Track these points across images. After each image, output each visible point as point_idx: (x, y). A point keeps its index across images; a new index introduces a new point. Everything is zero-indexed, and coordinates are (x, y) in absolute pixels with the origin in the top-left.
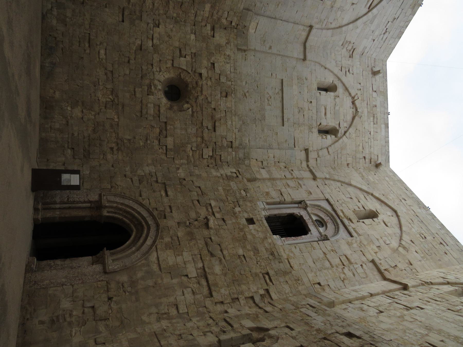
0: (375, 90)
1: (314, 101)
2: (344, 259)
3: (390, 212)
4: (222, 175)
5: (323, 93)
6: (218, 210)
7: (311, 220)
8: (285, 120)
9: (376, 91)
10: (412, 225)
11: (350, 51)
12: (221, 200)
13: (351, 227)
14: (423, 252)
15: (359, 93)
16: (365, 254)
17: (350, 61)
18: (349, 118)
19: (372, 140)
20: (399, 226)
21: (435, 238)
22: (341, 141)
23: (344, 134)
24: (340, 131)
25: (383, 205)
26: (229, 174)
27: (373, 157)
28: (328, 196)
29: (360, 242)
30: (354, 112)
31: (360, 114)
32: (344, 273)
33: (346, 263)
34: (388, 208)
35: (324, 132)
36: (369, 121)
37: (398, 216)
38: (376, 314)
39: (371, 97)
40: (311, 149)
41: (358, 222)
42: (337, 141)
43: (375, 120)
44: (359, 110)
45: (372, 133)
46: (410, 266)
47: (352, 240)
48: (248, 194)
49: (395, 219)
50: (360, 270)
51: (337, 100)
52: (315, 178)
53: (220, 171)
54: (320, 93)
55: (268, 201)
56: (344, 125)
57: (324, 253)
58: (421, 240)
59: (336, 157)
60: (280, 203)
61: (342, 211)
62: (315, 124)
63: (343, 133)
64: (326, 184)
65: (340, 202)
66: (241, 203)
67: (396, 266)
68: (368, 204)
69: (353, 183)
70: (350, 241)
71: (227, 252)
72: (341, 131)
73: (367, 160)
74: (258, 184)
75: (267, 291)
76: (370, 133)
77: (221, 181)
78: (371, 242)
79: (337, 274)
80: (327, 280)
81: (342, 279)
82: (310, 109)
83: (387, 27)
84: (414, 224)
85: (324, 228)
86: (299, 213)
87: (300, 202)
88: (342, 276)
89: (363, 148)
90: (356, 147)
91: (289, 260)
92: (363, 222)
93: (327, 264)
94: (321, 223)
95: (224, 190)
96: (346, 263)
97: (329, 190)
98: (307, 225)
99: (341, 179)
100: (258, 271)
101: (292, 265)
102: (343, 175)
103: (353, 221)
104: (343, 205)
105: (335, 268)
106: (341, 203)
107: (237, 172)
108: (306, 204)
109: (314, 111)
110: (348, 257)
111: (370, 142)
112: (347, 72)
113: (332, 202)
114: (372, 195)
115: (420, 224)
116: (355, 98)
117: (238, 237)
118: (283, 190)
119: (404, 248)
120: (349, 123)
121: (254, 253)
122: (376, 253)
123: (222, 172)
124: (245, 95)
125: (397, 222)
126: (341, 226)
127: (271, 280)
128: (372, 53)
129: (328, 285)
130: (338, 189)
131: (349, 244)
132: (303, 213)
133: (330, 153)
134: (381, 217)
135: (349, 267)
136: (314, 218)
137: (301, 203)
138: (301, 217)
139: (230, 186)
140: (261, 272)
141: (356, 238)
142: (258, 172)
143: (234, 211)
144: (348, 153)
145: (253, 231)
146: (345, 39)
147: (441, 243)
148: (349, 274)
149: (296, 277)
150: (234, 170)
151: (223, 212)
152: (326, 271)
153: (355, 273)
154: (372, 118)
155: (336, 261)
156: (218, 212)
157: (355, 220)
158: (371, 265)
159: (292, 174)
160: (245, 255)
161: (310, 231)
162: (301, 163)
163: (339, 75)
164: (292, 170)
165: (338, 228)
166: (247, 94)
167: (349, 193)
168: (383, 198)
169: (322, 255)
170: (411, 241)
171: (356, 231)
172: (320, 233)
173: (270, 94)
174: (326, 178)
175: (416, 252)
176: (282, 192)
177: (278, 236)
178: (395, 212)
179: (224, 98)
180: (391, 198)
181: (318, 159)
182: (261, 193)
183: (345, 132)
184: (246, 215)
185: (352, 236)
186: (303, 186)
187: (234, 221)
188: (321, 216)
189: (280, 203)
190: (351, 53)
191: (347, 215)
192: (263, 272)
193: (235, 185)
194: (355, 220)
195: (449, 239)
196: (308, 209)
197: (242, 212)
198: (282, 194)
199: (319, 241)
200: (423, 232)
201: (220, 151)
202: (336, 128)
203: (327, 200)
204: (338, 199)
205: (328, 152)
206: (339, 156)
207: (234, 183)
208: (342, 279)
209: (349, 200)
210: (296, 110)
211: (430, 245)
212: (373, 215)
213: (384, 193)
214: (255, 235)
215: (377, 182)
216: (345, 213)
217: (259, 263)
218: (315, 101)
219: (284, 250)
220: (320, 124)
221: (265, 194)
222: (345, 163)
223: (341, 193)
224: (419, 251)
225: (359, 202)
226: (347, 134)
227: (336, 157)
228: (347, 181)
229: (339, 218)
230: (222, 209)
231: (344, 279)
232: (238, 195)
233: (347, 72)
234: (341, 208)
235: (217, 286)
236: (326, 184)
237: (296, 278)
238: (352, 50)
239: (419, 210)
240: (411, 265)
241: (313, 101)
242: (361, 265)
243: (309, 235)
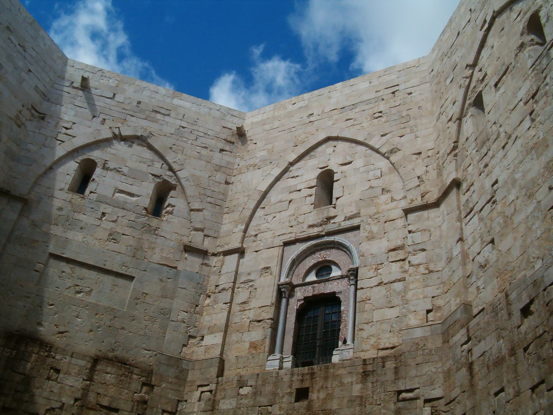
0: (111, 96)
1: (104, 208)
2: (394, 256)
3: (327, 148)
5: (91, 186)
7: (316, 285)
8: (123, 272)
9: (114, 95)
10: (356, 123)
11: (33, 115)
13: (340, 222)
14: (402, 126)
15: (109, 123)
16: (391, 218)
17: (49, 121)
18: (147, 154)
19: (195, 128)
20: (354, 145)
21: (384, 97)
22: (183, 181)
23: (174, 172)
24: (166, 178)
25: (312, 154)
27: (224, 137)
28: (279, 241)
29: (371, 217)
30: (140, 142)
31: (145, 135)
32: (418, 265)
33: (401, 255)
34: (320, 149)
35: (158, 206)
36: (161, 122)
37: (337, 139)
38: (495, 252)
39: (123, 106)
40: (186, 240)
41: (335, 208)
42: (183, 188)
43: (163, 111)
44: (139, 134)
45: (184, 124)
46: (423, 156)
47: (364, 229)
49: (341, 145)
50: (418, 237)
51: (111, 165)
52: (241, 252)
54: (91, 192)
55: (267, 349)
56: (158, 167)
57: (380, 284)
58: (383, 119)
59: (209, 199)
60: (274, 328)
61: (311, 226)
62: (143, 220)
63: (170, 173)
64: (256, 235)
65: (294, 223)
67: (419, 177)
68: (305, 178)
69: (263, 187)
70: (366, 234)
72: (167, 175)
73: (227, 148)
74: (230, 356)
75: (427, 401)
76: (184, 128)
78: (372, 200)
79: (417, 277)
80: (425, 297)
81: (427, 272)
82: (115, 218)
83: (17, 44)
84: (355, 120)
85: (333, 267)
86: (299, 300)
87: (280, 294)
88: (422, 269)
89: (206, 148)
90: (200, 159)
91: (381, 347)
92: (337, 199)
93: (398, 286)
94: (323, 269)
96: (401, 255)
97: (269, 235)
98: (323, 294)
99: (252, 205)
100: (392, 406)
101: (391, 346)
102: (246, 198)
103: (332, 214)
104: (300, 219)
105: (406, 275)
106: (295, 223)
107: (201, 389)
108: (286, 284)
109: (121, 213)
110: (392, 248)
111: (197, 133)
112: (68, 132)
113: (292, 237)
114: (292, 164)
115: (357, 110)
116: (117, 133)
118: (251, 315)
119: (392, 151)
120: (156, 158)
122: (393, 200)
124: (62, 333)
125: (347, 144)
126: (337, 238)
127: (411, 391)
128: (48, 79)
129: (433, 297)
130: (270, 218)
131: (371, 238)
132: (300, 294)
133: (201, 207)
134: (333, 166)
135: (409, 252)
136: (312, 277)
137: (284, 292)
138: (306, 299)
140: (395, 403)
141: (362, 221)
142: (207, 348)
144: (207, 176)
146: (11, 118)
147: (393, 93)
148: (420, 258)
149: (412, 347)
150: (197, 394)
152: (410, 295)
153: (420, 247)
154: (159, 116)
155: (394, 270)
157: (332, 212)
158: (411, 217)
159: (224, 289)
161: (334, 293)
162: (206, 265)
163: (70, 149)
164: (217, 286)
166: (62, 329)
167: (280, 201)
168: (301, 150)
169: (382, 290)
170: (382, 136)
171: (350, 218)
172: (342, 277)
173: (69, 284)
174: (245, 231)
175: (401, 137)
176: (255, 319)
177: (334, 352)
178: (328, 139)
179: (61, 375)
180: (303, 136)
181: (206, 232)
182: (251, 357)
183: (171, 169)
185: (357, 228)
186: (251, 277)
188: (311, 264)
189: (274, 328)
190: (36, 114)
191: (319, 221)
192: (395, 399)
193: (227, 401)
194: (332, 212)
195: (387, 78)
196: (295, 282)
198: (259, 321)
199: (356, 285)
200: (371, 112)
201: (155, 410)
202: (158, 182)
203: (287, 244)
204: (287, 224)
205: (198, 210)
206: (209, 193)
208: (427, 272)
209: (292, 206)
210: (111, 245)
211: (394, 110)
212: (327, 180)
213: (292, 144)
215: (269, 146)
216: (315, 222)
218: (103, 206)
219: (363, 351)
220: (146, 209)
221: (254, 352)
222: (223, 186)
223: (278, 215)
224: (401, 132)
225: (300, 190)
226: (175, 167)
227: (209, 199)
228: (257, 197)
229: (323, 236)
231: (427, 269)
233: (68, 132)
234: (305, 226)
236: (256, 235)
237: (414, 347)
238: (33, 111)
239: (333, 101)
240: (420, 153)
241: (102, 210)
242: (410, 232)
243: (341, 297)
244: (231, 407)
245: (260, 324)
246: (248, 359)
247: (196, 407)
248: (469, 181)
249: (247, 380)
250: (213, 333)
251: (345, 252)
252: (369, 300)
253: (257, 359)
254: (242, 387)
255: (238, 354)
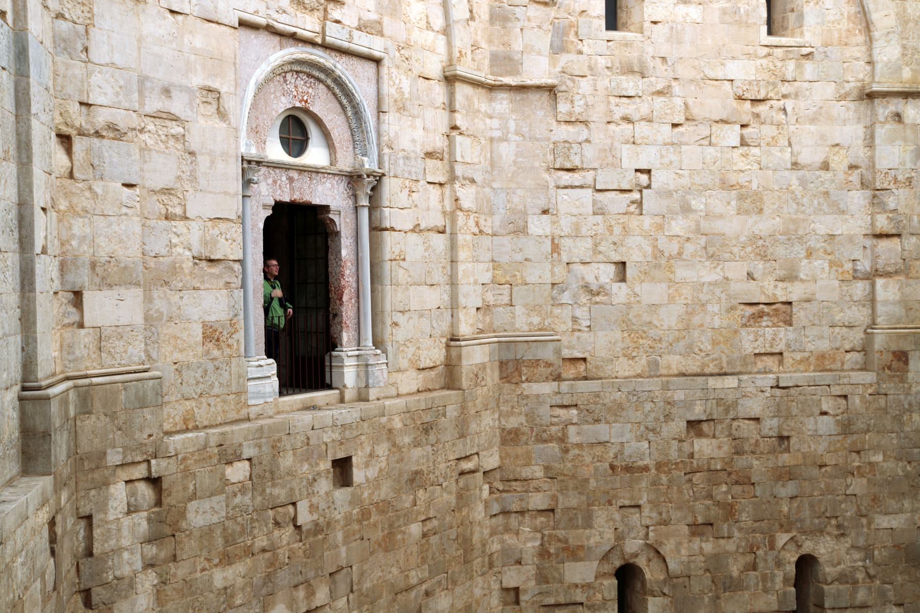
4: (149, 565)
6: (301, 593)
12: (269, 578)
26: (141, 522)
48: (248, 452)
53: (126, 571)
66: (280, 493)
71: (413, 573)
77: (180, 571)
95: (227, 560)
117: (383, 531)
121: (420, 487)
123: (129, 562)
139: (208, 532)
143: (308, 531)
145: (372, 473)
151: (311, 574)
156: (311, 593)
160: (423, 518)
161: (325, 209)
165: (338, 81)
184: (324, 485)
187: (340, 536)
193: (206, 504)
197: (315, 500)
207: (192, 506)
214: (381, 470)
217: (441, 480)
221: (216, 353)
230: (300, 578)
232: (247, 499)
235: (470, 605)
244: (215, 519)
245: (216, 270)
246: (206, 371)
247: (125, 532)
248: (577, 109)
249: (240, 445)
250: (110, 286)
251: (343, 108)
252: (404, 260)
253: (226, 375)
254: (230, 463)
255: (177, 356)
